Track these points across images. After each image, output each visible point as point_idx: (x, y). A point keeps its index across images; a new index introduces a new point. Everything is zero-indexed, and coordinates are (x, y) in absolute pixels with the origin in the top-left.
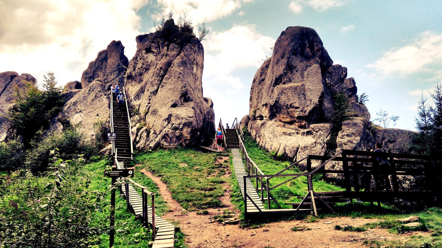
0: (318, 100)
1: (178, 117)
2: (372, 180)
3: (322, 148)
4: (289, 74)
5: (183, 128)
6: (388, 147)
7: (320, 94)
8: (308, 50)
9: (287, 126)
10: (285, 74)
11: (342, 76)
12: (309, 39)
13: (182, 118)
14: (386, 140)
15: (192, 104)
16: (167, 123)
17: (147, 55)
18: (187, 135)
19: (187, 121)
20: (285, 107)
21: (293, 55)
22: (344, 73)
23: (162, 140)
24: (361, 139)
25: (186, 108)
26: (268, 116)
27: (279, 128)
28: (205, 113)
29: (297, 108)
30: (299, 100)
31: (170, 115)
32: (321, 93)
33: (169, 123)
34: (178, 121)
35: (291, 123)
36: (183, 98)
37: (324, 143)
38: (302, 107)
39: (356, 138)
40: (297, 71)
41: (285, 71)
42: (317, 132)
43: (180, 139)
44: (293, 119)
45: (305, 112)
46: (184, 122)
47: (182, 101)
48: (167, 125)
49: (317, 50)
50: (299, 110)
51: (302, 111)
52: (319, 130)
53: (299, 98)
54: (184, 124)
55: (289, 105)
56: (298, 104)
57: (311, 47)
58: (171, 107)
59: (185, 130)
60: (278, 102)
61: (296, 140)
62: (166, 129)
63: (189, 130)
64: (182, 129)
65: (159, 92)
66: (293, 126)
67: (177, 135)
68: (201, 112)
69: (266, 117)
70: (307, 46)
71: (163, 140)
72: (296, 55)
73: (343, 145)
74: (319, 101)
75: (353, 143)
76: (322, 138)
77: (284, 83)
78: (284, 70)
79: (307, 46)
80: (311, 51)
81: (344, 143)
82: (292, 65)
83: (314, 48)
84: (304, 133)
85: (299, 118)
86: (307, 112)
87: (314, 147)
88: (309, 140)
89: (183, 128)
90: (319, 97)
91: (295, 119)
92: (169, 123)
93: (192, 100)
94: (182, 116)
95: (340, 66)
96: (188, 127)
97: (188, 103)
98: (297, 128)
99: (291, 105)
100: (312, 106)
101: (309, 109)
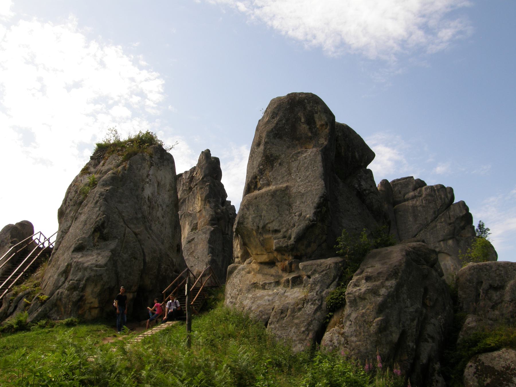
0: (313, 211)
1: (79, 267)
2: (436, 377)
3: (316, 311)
4: (267, 172)
5: (85, 286)
6: (490, 299)
7: (316, 200)
8: (304, 128)
9: (267, 269)
10: (261, 172)
11: (446, 199)
12: (305, 109)
13: (86, 269)
14: (485, 286)
15: (113, 245)
16: (63, 279)
17: (82, 178)
18: (93, 300)
19: (93, 274)
20: (254, 233)
21: (274, 138)
22: (449, 196)
23: (51, 310)
24: (399, 286)
25: (99, 251)
26: (239, 255)
27: (250, 276)
28: (148, 259)
29: (276, 231)
30: (281, 215)
31: (69, 265)
32: (321, 197)
33: (66, 279)
34: (80, 274)
35: (271, 263)
36: (98, 234)
37: (322, 299)
38: (284, 230)
39: (388, 283)
40: (280, 164)
41: (261, 167)
42: (309, 277)
43: (80, 307)
44: (272, 256)
45: (290, 238)
46: (87, 275)
47: (96, 239)
48: (64, 282)
49: (322, 125)
50: (280, 235)
51: (284, 237)
52: (313, 274)
53: (278, 212)
54: (88, 280)
55: (261, 226)
56: (277, 225)
57: (310, 121)
58: (73, 251)
59: (89, 290)
60: (242, 223)
61: (270, 298)
62: (60, 290)
63: (97, 289)
64: (83, 289)
65: (71, 229)
66: (273, 271)
67: (74, 300)
68: (136, 258)
69: (238, 257)
70: (303, 120)
71: (54, 310)
72: (281, 138)
73: (358, 300)
74: (315, 214)
75: (379, 295)
76: (318, 288)
77: (259, 189)
78: (259, 167)
79: (303, 120)
80: (310, 129)
81: (359, 297)
82: (271, 155)
83: (315, 123)
84: (288, 281)
85: (279, 250)
86: (292, 239)
87: (300, 309)
88: (296, 294)
89: (85, 286)
90: (315, 205)
91: (275, 254)
92: (66, 279)
93: (116, 237)
94: (86, 265)
95: (442, 187)
96: (96, 285)
97: (107, 242)
98: (280, 272)
99: (264, 227)
100: (303, 225)
101: (294, 233)
